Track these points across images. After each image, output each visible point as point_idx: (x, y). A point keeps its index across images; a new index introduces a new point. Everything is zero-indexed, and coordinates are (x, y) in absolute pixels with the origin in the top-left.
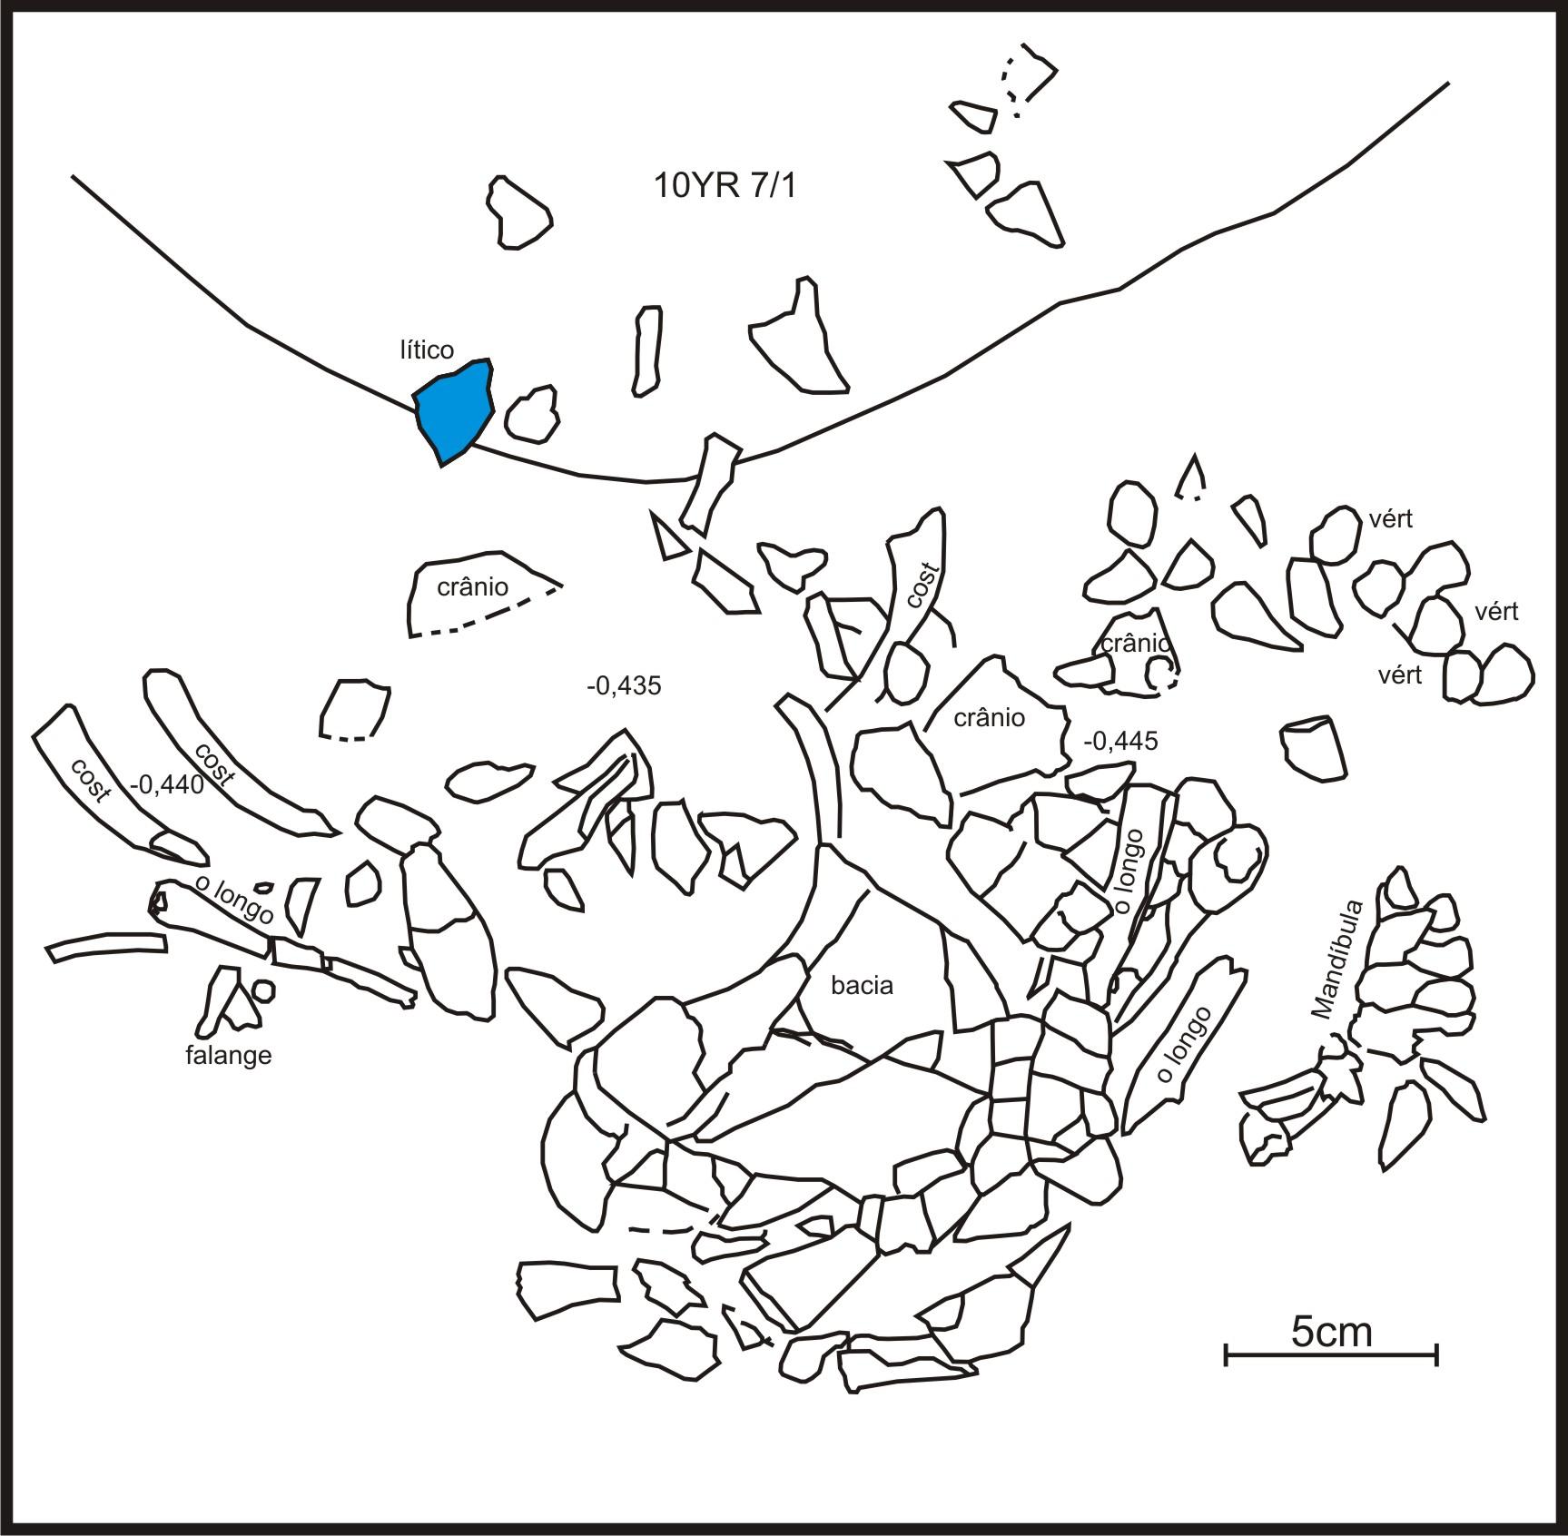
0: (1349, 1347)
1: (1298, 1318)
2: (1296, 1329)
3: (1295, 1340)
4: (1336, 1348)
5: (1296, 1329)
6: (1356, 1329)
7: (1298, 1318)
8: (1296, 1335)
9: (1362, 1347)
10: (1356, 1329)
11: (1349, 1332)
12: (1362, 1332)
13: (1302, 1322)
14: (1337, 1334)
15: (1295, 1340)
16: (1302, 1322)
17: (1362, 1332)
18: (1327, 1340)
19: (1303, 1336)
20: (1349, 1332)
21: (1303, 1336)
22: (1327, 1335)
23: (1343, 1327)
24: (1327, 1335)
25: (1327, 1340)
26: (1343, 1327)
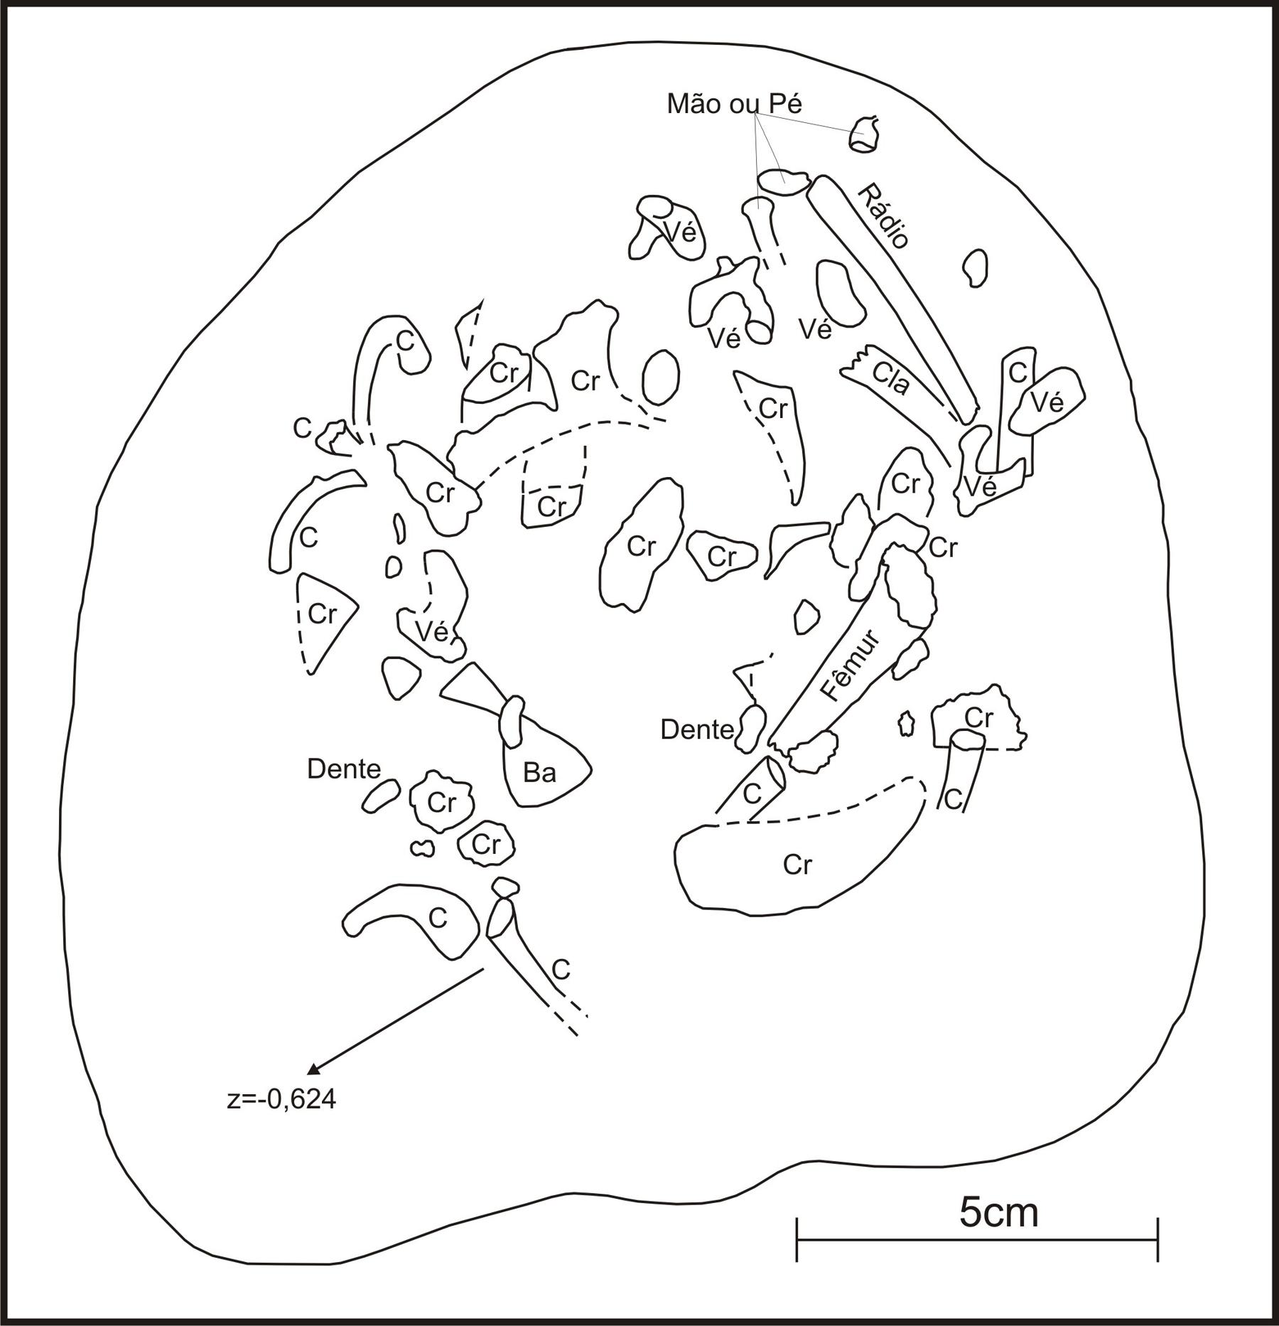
1: (966, 1198)
2: (964, 1209)
3: (963, 1220)
5: (964, 1209)
6: (1022, 1209)
7: (966, 1198)
8: (964, 1215)
10: (1022, 1209)
11: (1016, 1212)
12: (1029, 1212)
13: (970, 1203)
14: (1004, 1215)
15: (963, 1220)
16: (970, 1203)
17: (1029, 1212)
18: (994, 1220)
19: (971, 1216)
20: (1016, 1212)
21: (971, 1216)
23: (1010, 1208)
24: (995, 1215)
25: (994, 1220)
26: (1010, 1208)
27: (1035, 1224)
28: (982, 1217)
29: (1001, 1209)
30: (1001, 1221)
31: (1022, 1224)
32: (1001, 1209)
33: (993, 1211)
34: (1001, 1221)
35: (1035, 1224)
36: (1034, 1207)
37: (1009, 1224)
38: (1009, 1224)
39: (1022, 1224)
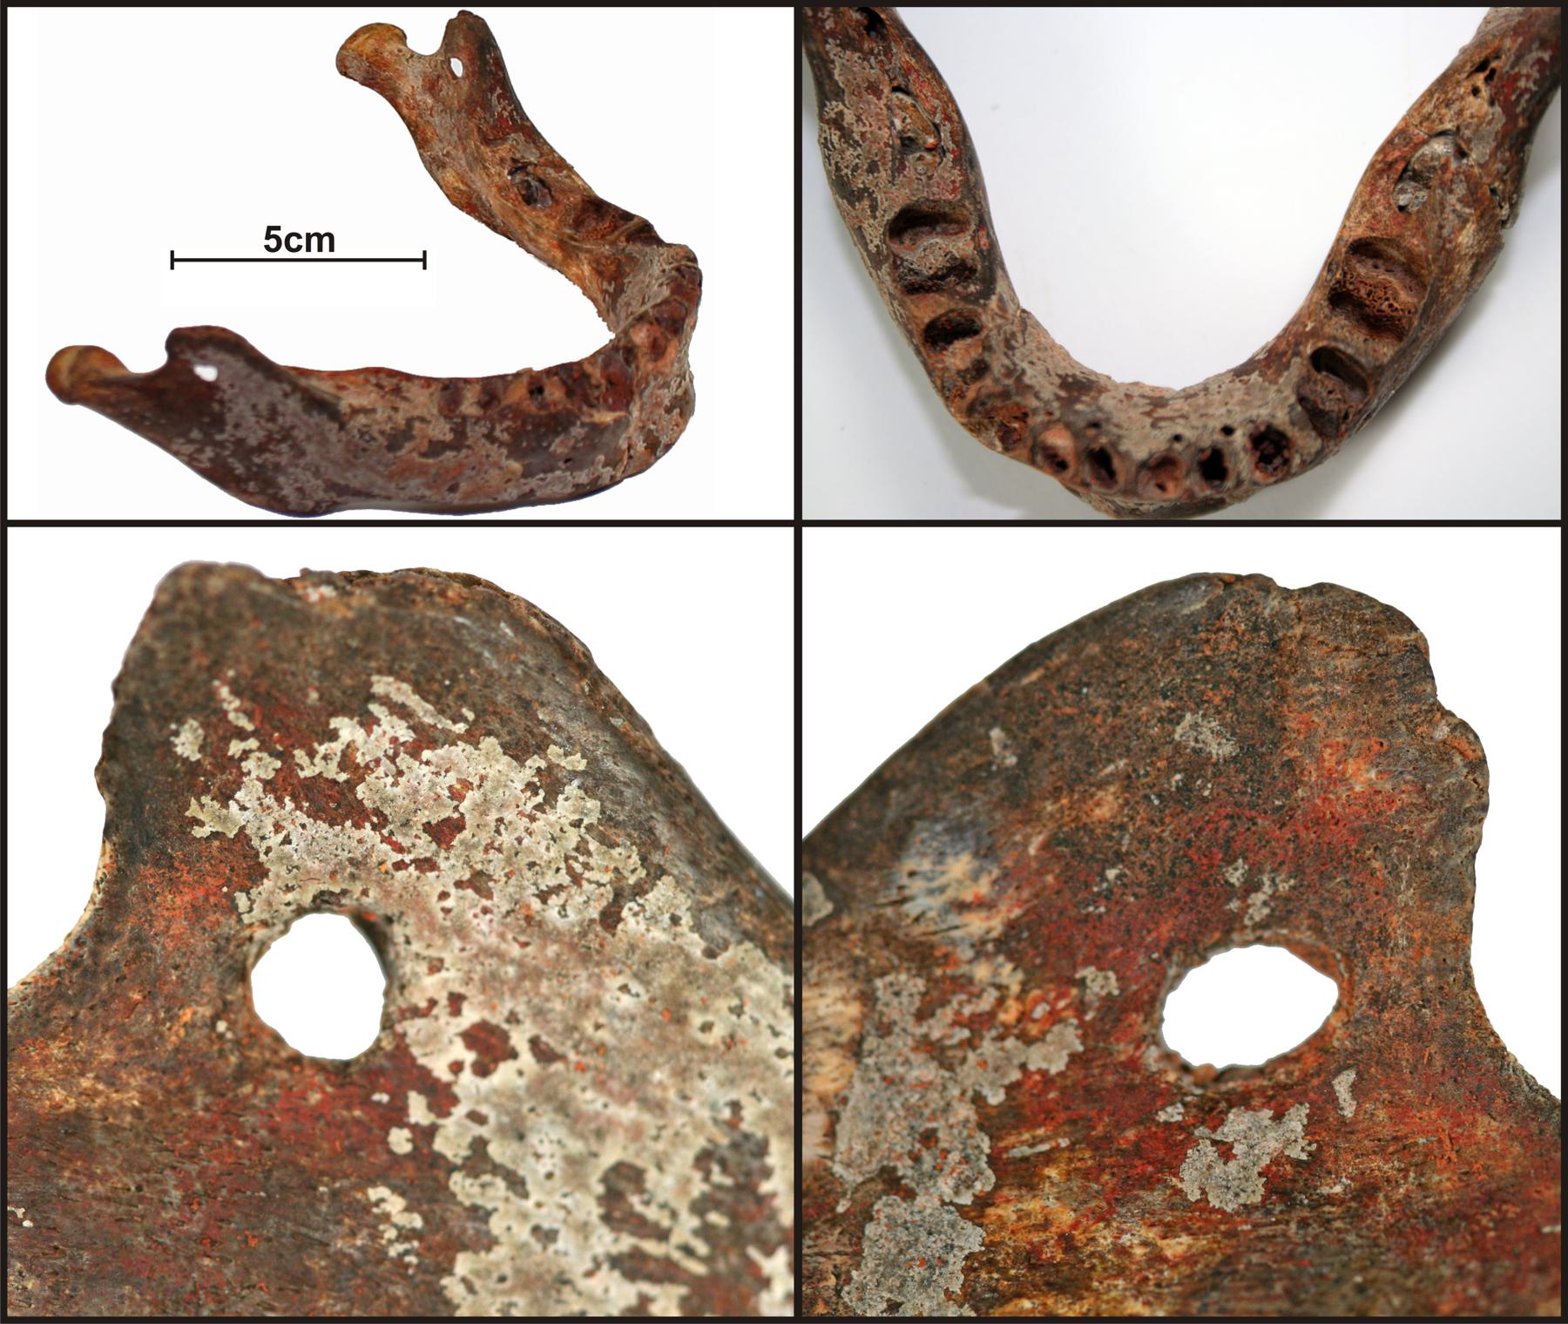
0: (314, 254)
1: (270, 228)
4: (302, 254)
5: (268, 237)
7: (270, 228)
9: (326, 254)
11: (314, 240)
12: (326, 240)
14: (303, 242)
17: (326, 240)
19: (273, 243)
20: (314, 240)
21: (273, 243)
22: (294, 242)
24: (294, 242)
26: (309, 236)
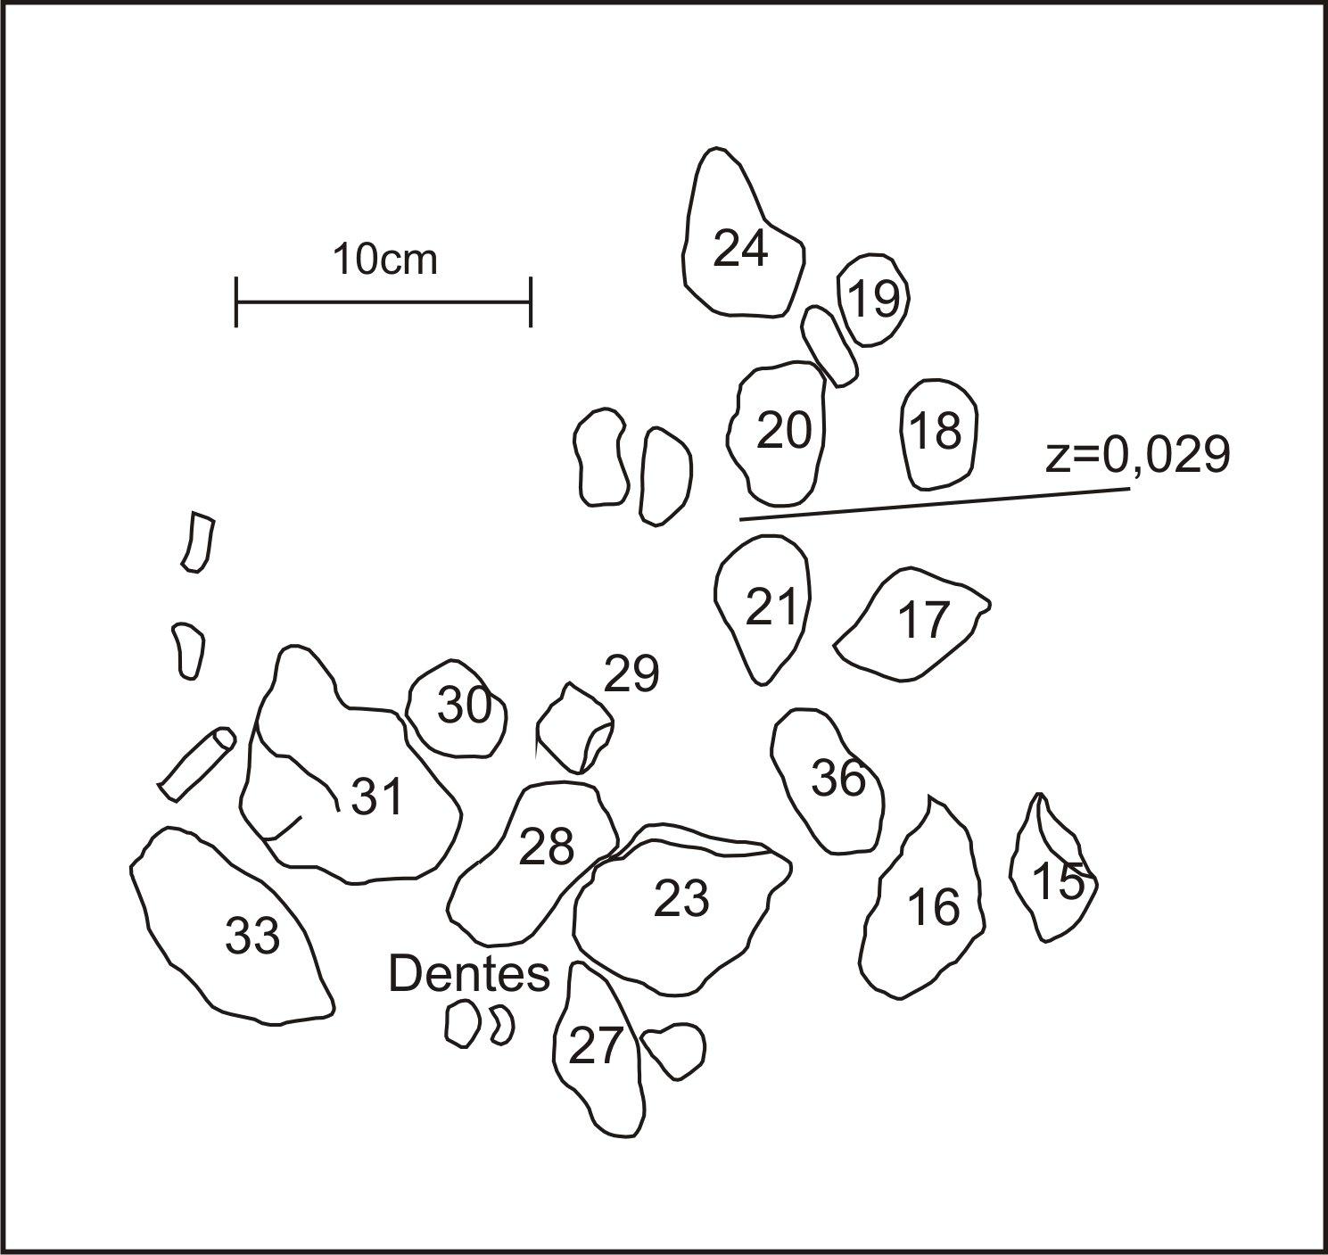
6: (421, 256)
10: (421, 256)
11: (414, 259)
12: (427, 259)
14: (401, 261)
17: (427, 259)
18: (391, 268)
20: (414, 259)
22: (392, 262)
23: (407, 255)
24: (392, 262)
25: (391, 268)
26: (407, 255)
27: (434, 272)
28: (380, 261)
29: (398, 256)
30: (399, 268)
31: (420, 272)
32: (398, 256)
33: (391, 257)
34: (399, 268)
35: (434, 272)
36: (432, 253)
37: (407, 272)
38: (407, 272)
39: (420, 272)
